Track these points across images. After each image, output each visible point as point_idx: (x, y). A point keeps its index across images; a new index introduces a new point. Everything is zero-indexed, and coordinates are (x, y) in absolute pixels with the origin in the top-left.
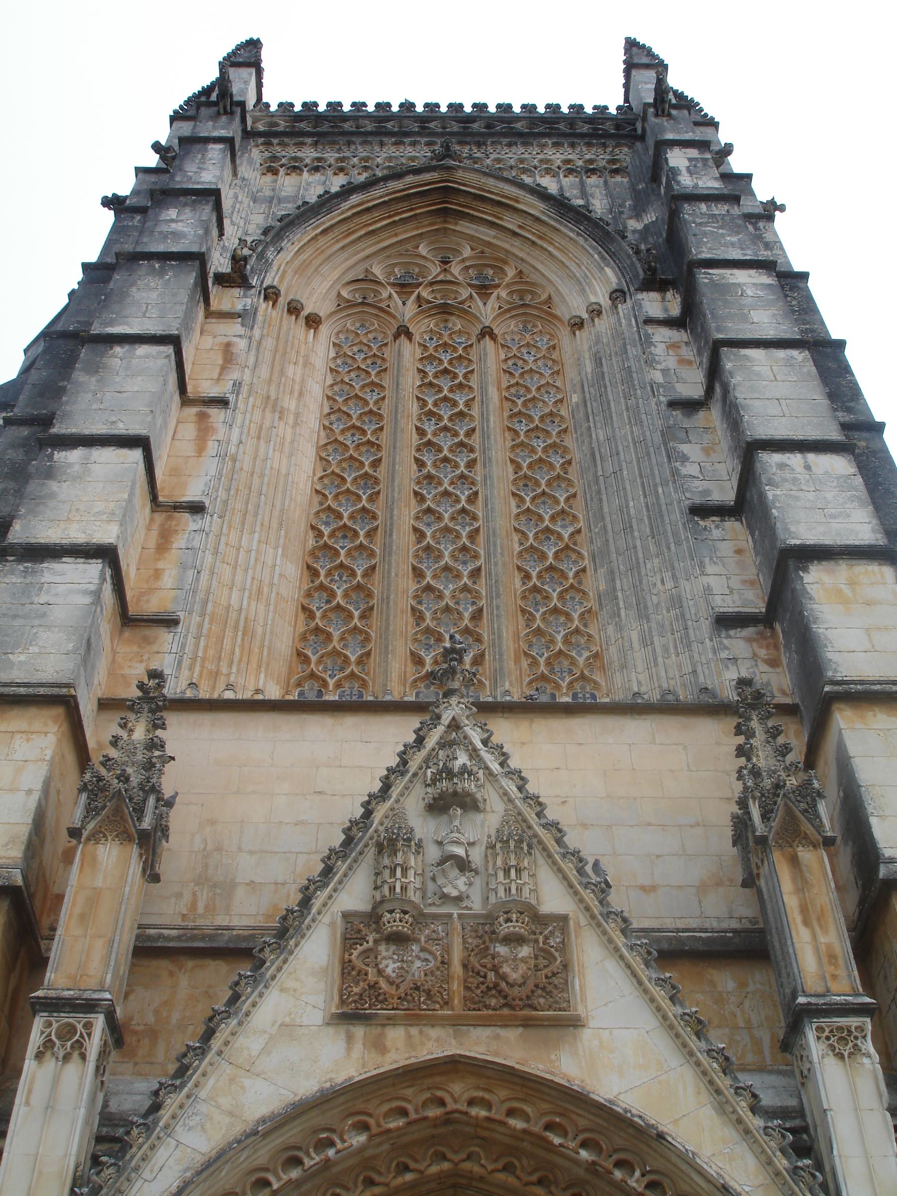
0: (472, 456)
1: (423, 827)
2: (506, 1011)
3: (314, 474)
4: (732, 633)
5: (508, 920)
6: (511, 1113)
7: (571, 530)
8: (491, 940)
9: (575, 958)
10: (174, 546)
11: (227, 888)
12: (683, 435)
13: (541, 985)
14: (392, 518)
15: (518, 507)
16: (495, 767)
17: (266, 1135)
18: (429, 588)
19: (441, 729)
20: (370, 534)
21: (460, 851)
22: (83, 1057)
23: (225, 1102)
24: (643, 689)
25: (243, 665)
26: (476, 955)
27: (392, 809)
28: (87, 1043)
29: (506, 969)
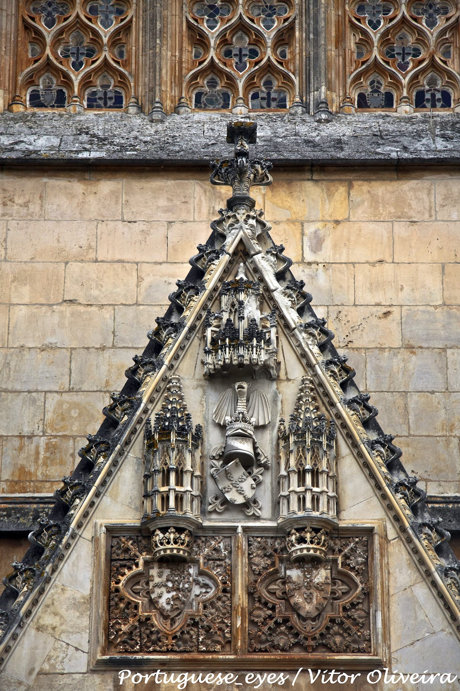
2: (297, 654)
5: (302, 540)
8: (281, 561)
9: (379, 586)
13: (338, 621)
16: (292, 316)
19: (225, 258)
21: (245, 447)
26: (262, 581)
27: (164, 379)
29: (298, 599)
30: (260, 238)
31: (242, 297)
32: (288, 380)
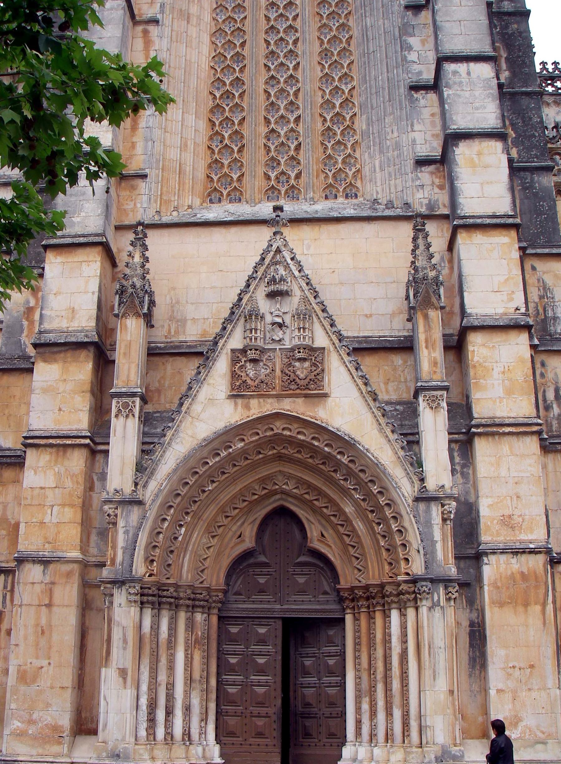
0: (298, 35)
1: (264, 305)
2: (298, 391)
3: (210, 55)
4: (423, 169)
5: (299, 352)
6: (299, 433)
7: (350, 86)
9: (327, 367)
10: (140, 126)
11: (183, 322)
12: (411, 30)
14: (252, 86)
15: (322, 71)
16: (296, 273)
17: (206, 446)
18: (273, 131)
19: (272, 253)
20: (241, 96)
21: (279, 320)
22: (133, 415)
23: (190, 432)
24: (379, 196)
25: (181, 192)
27: (251, 297)
28: (134, 410)
29: (298, 373)
30: (285, 246)
31: (278, 266)
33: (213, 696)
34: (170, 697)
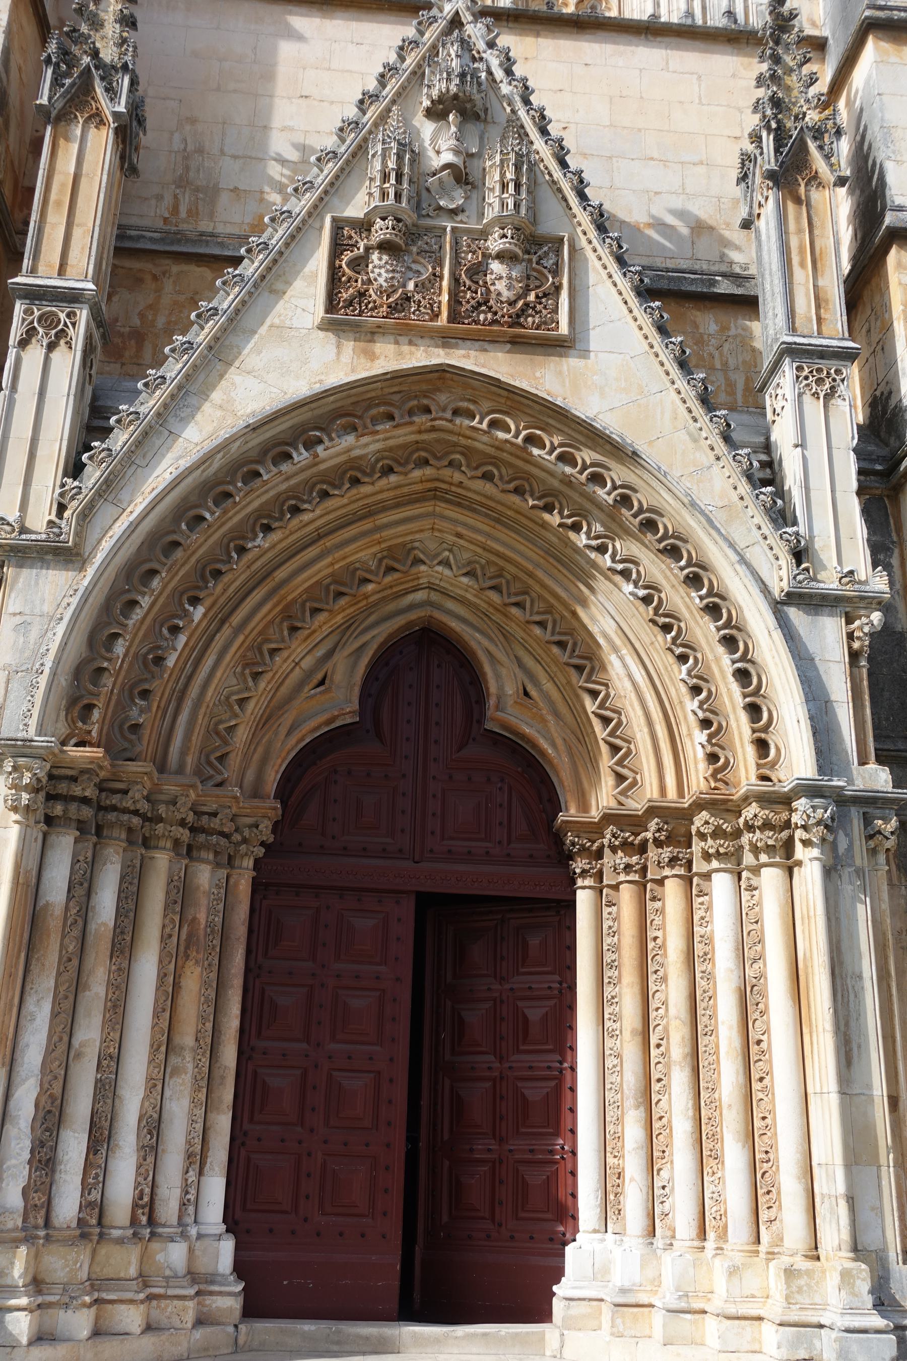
22: (69, 344)
27: (388, 110)
28: (71, 331)
32: (494, 123)
33: (227, 1094)
34: (107, 1090)
